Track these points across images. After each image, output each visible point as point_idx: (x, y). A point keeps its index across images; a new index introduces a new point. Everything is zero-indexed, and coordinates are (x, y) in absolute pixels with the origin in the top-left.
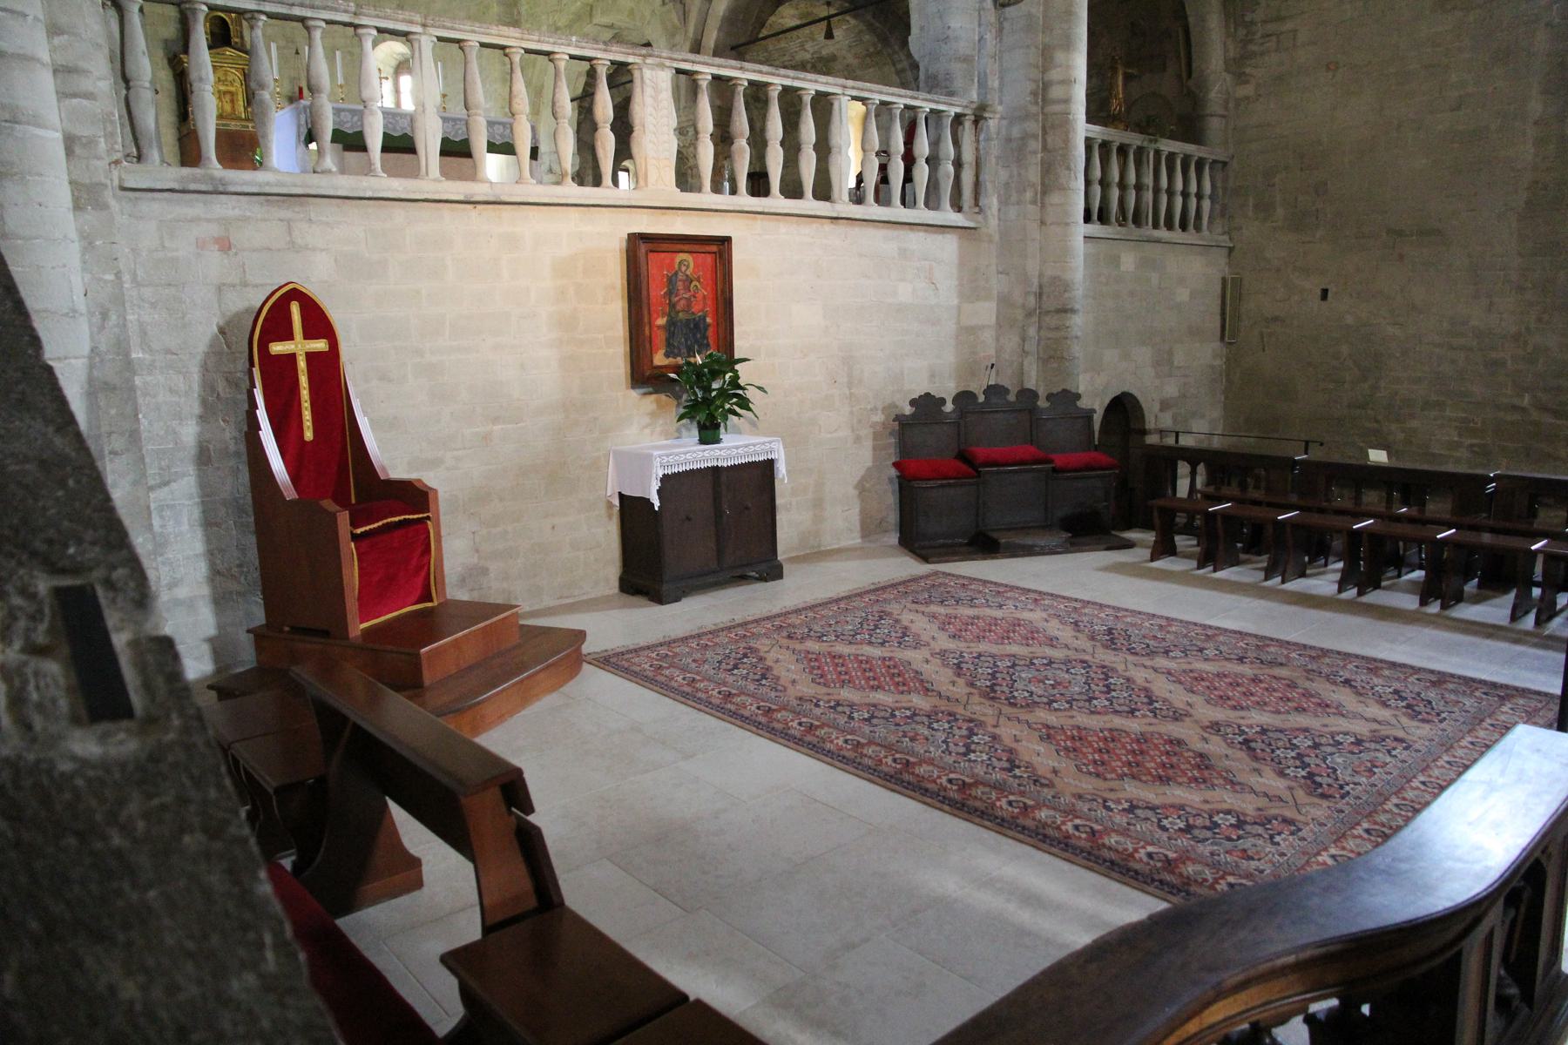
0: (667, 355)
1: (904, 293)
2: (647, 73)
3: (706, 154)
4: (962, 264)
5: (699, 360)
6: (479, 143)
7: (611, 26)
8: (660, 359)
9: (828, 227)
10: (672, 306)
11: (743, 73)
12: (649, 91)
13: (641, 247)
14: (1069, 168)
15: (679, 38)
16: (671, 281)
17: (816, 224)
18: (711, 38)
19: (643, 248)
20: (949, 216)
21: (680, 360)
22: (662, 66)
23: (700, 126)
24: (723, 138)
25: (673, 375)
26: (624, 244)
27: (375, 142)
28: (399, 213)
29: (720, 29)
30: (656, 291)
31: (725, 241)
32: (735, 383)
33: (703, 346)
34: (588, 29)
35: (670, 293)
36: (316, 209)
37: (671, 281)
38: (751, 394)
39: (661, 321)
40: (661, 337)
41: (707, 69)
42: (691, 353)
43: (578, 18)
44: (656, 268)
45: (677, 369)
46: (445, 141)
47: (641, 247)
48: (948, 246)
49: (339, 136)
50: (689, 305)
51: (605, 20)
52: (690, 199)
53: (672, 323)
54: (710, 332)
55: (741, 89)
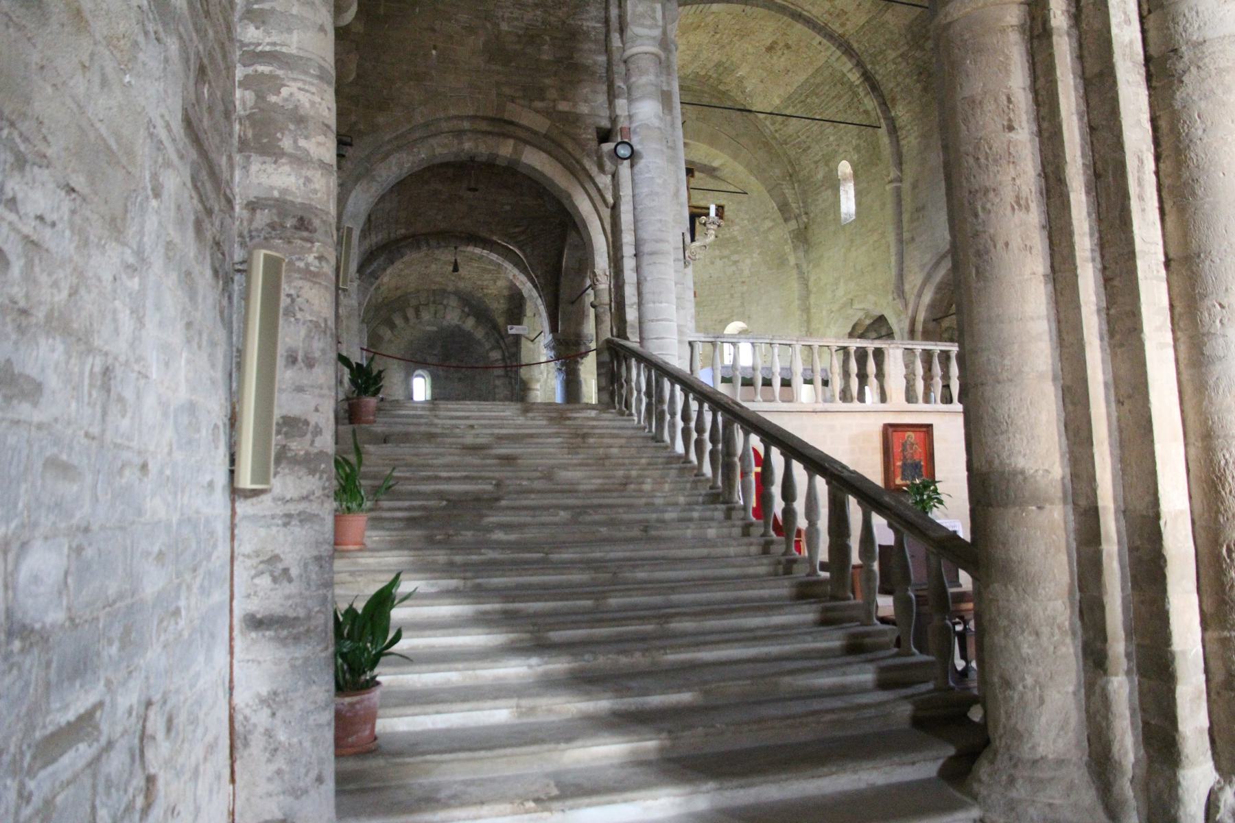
0: (902, 479)
2: (891, 351)
3: (920, 386)
5: (918, 481)
6: (798, 380)
7: (864, 309)
8: (898, 481)
10: (905, 457)
11: (937, 347)
12: (892, 359)
13: (890, 431)
15: (903, 316)
16: (904, 445)
18: (919, 327)
19: (890, 430)
21: (908, 482)
22: (898, 348)
23: (917, 373)
24: (928, 377)
25: (905, 488)
26: (881, 429)
27: (759, 382)
29: (926, 311)
30: (897, 450)
31: (930, 426)
32: (935, 491)
33: (920, 476)
34: (850, 311)
35: (903, 451)
37: (904, 445)
38: (943, 497)
39: (899, 463)
40: (899, 471)
41: (919, 346)
42: (914, 478)
43: (844, 306)
44: (896, 439)
45: (907, 486)
47: (890, 431)
50: (913, 457)
51: (861, 306)
52: (912, 407)
53: (904, 465)
54: (923, 469)
55: (936, 355)
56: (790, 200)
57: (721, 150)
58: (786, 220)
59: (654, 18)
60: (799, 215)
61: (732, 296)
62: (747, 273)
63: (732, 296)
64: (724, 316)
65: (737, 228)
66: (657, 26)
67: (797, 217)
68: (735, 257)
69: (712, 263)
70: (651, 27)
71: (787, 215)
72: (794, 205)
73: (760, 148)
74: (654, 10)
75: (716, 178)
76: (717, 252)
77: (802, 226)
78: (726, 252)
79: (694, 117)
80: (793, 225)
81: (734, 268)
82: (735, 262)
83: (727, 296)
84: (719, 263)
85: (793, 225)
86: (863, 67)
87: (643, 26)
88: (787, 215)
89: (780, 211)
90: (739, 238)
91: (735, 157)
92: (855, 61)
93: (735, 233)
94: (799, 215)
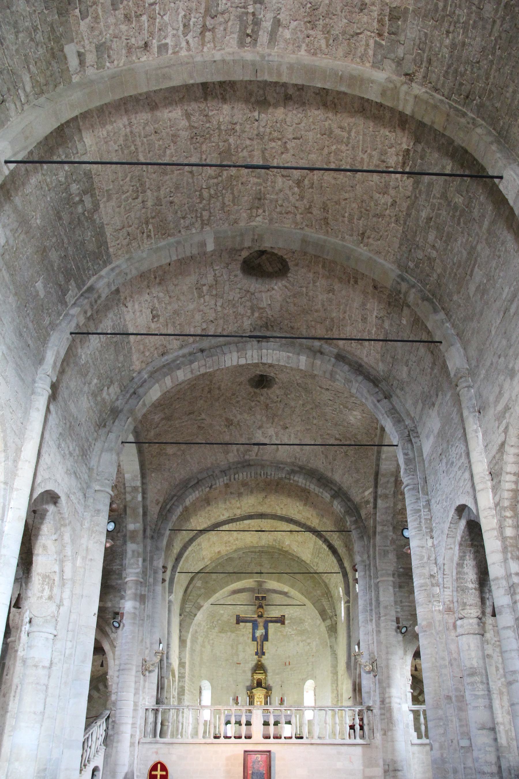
1: (339, 765)
4: (364, 755)
9: (309, 746)
14: (392, 723)
17: (305, 746)
20: (358, 741)
28: (191, 746)
30: (250, 765)
31: (269, 752)
36: (174, 746)
46: (264, 721)
48: (359, 750)
49: (236, 723)
56: (327, 608)
57: (284, 584)
58: (324, 620)
59: (138, 564)
60: (332, 616)
61: (308, 664)
62: (314, 650)
63: (308, 664)
64: (304, 677)
65: (307, 624)
66: (138, 568)
67: (331, 618)
68: (309, 641)
69: (298, 644)
70: (135, 569)
71: (324, 617)
72: (329, 611)
73: (308, 580)
74: (138, 561)
75: (288, 597)
76: (300, 638)
77: (334, 623)
78: (304, 638)
79: (269, 567)
80: (328, 622)
81: (308, 647)
82: (309, 644)
83: (306, 664)
84: (301, 644)
85: (328, 622)
86: (328, 542)
87: (132, 568)
88: (324, 617)
89: (320, 615)
90: (309, 629)
91: (292, 586)
92: (323, 539)
93: (307, 627)
94: (332, 616)
